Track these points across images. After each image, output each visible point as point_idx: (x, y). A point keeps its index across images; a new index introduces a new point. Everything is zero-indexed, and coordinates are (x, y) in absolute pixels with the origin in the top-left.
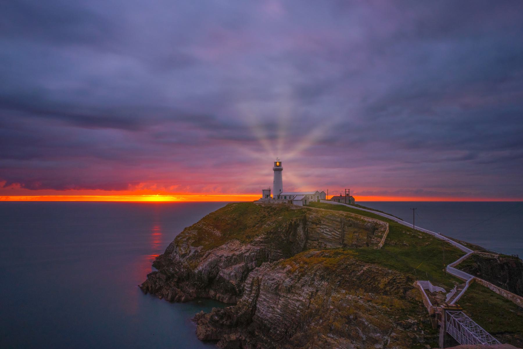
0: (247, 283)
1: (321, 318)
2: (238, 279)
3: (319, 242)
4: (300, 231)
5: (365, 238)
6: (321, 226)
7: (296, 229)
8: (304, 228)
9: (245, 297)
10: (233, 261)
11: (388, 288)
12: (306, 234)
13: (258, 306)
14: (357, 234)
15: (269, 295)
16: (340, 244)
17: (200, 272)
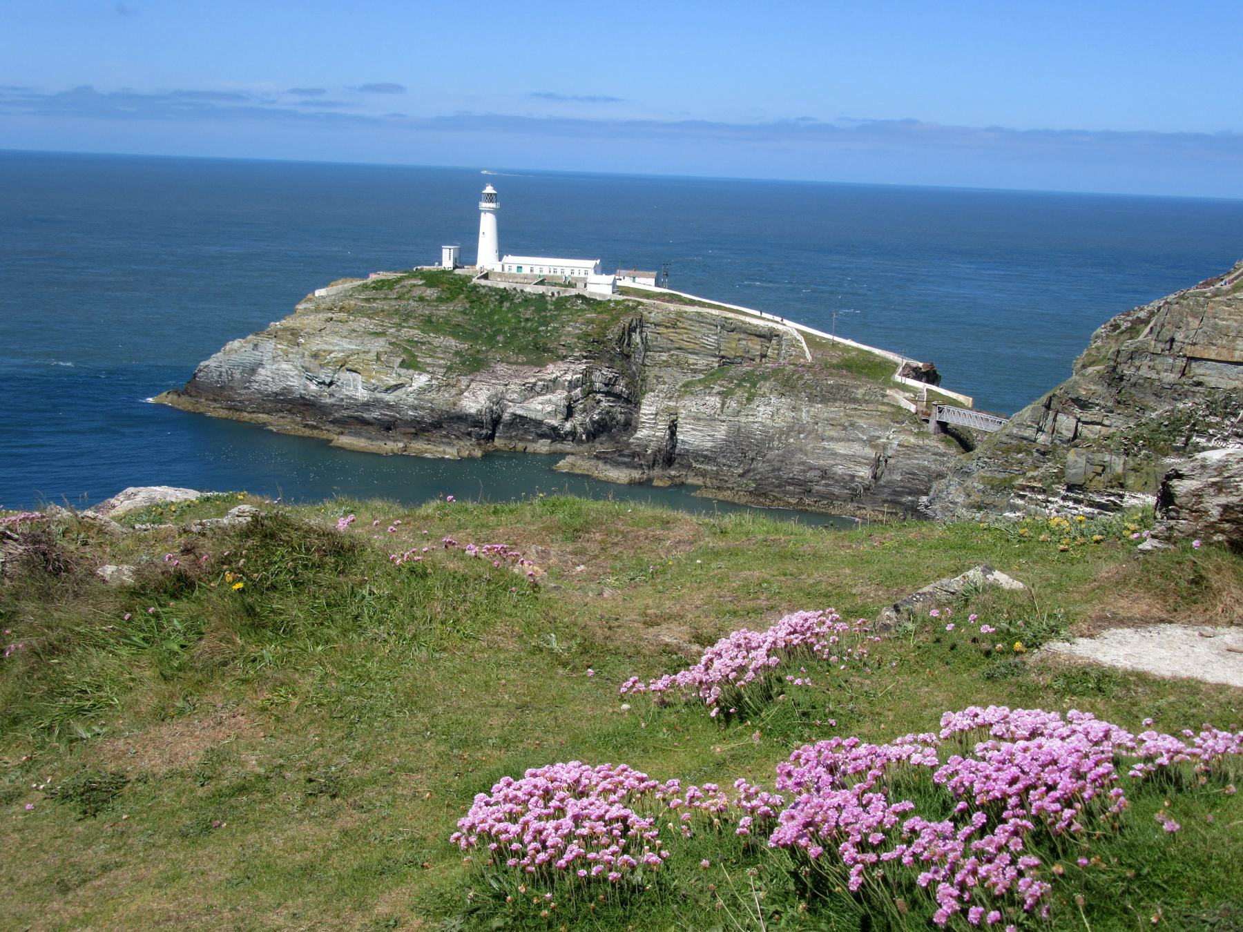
0: (645, 414)
1: (799, 433)
2: (560, 417)
3: (672, 355)
4: (636, 338)
5: (759, 347)
6: (678, 331)
7: (630, 336)
8: (641, 332)
9: (640, 434)
10: (538, 389)
11: (867, 398)
12: (644, 341)
13: (680, 437)
14: (744, 342)
15: (702, 423)
16: (715, 356)
17: (480, 411)
